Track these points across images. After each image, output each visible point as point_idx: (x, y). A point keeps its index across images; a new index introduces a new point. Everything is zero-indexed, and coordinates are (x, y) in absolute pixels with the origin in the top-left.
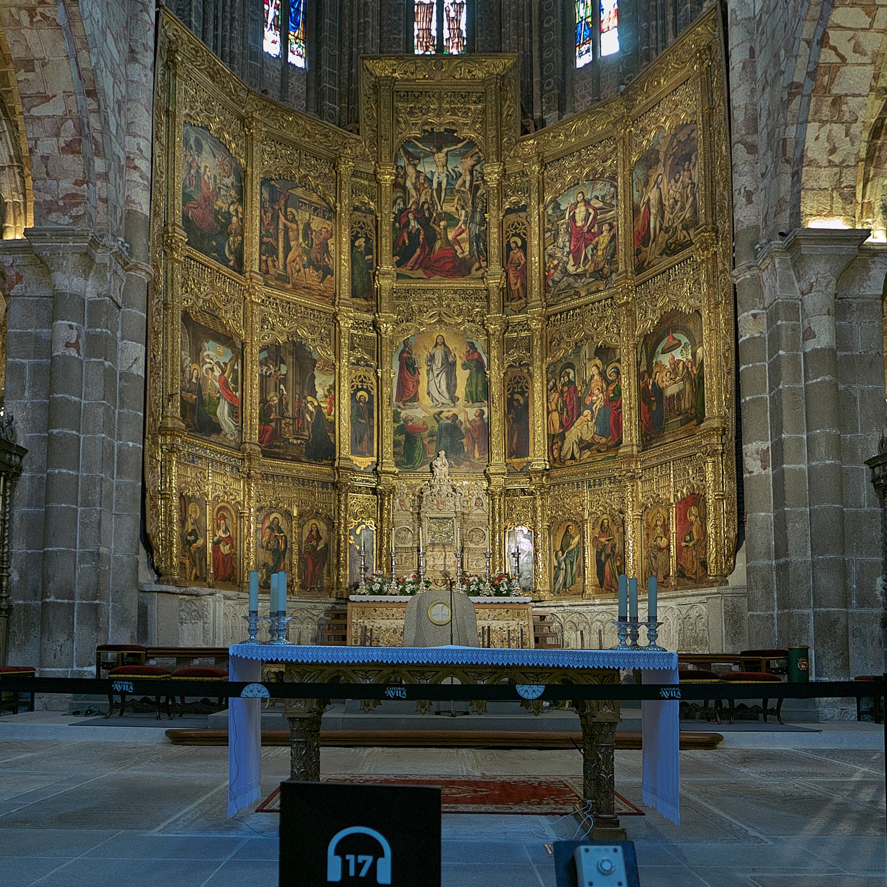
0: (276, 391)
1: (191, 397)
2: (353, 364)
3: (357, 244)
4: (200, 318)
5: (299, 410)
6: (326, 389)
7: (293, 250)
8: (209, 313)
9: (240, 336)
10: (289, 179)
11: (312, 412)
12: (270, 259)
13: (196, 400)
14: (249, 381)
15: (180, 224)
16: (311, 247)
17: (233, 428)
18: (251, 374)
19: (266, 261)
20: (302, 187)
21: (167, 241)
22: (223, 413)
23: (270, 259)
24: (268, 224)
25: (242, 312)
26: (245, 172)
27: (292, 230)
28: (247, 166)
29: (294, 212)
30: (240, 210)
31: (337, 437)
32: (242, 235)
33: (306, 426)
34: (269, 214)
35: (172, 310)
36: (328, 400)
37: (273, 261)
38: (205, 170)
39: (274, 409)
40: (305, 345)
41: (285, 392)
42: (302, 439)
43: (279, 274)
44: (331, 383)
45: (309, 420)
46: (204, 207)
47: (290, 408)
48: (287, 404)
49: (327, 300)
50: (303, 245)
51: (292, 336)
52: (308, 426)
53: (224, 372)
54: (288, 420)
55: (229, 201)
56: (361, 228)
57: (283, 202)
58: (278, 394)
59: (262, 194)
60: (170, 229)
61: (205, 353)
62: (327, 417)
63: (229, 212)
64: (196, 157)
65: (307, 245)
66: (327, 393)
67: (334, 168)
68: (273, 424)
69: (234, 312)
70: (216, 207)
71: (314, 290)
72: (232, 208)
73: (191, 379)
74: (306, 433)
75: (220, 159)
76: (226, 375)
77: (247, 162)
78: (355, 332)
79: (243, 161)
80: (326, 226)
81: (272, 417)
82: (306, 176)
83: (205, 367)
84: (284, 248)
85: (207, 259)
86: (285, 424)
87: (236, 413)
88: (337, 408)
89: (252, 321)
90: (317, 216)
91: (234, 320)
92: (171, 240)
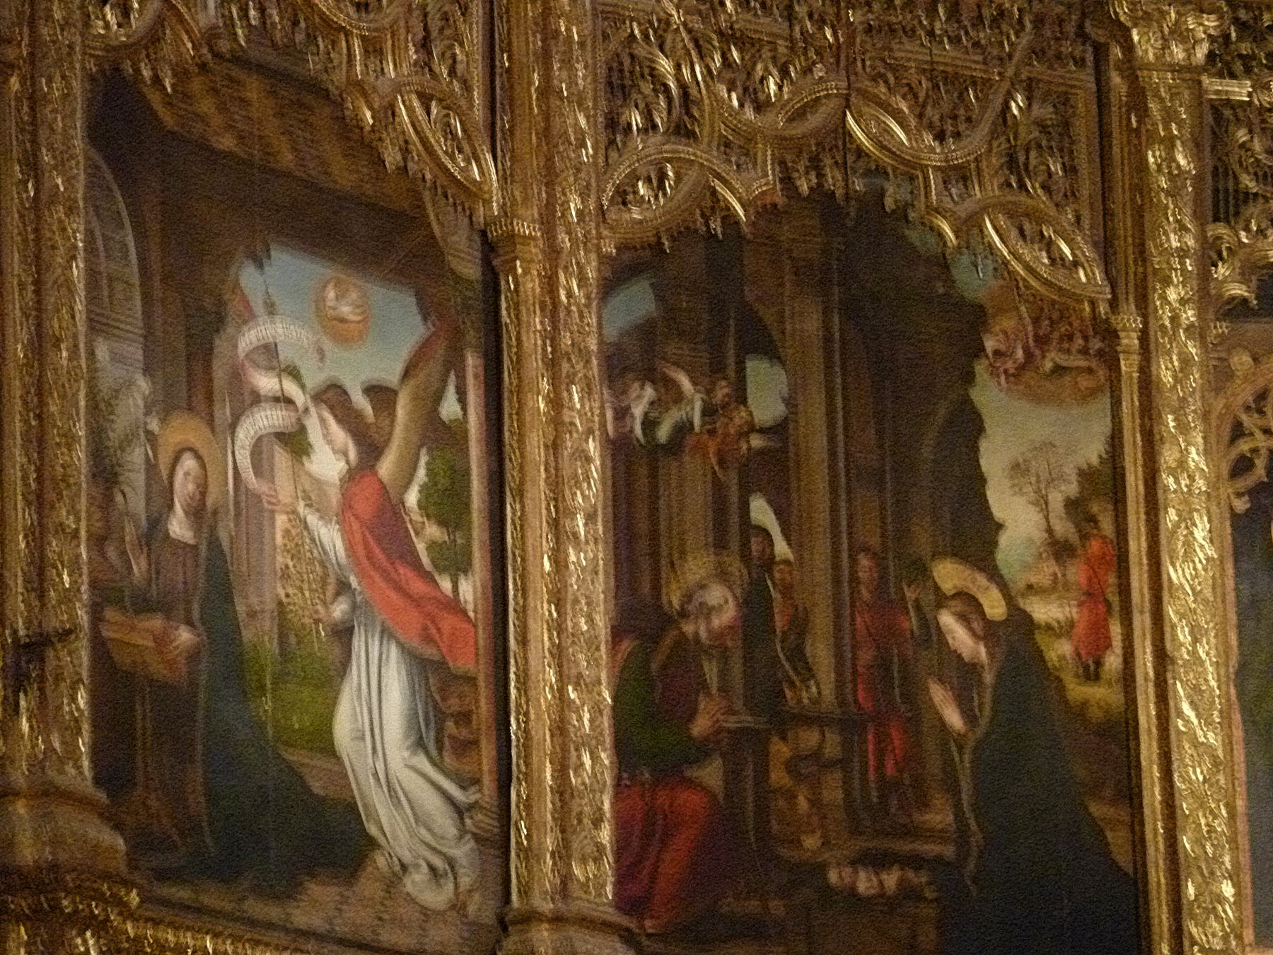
0: (720, 544)
1: (162, 641)
2: (1236, 310)
4: (206, 106)
5: (883, 665)
6: (1056, 499)
8: (261, 69)
9: (469, 193)
11: (970, 670)
13: (193, 656)
14: (538, 489)
17: (445, 822)
18: (555, 447)
22: (375, 729)
25: (474, 35)
31: (1155, 827)
33: (934, 765)
35: (30, 80)
36: (1076, 572)
39: (711, 670)
40: (902, 214)
41: (781, 548)
42: (916, 862)
44: (1093, 452)
45: (954, 718)
47: (820, 652)
48: (800, 624)
51: (815, 165)
52: (948, 762)
53: (370, 447)
54: (810, 738)
58: (735, 566)
61: (249, 338)
62: (1077, 691)
66: (1063, 528)
68: (711, 774)
69: (425, 45)
73: (156, 523)
74: (939, 816)
76: (387, 467)
78: (1240, 90)
81: (701, 726)
83: (246, 434)
86: (792, 766)
87: (464, 718)
88: (1142, 621)
89: (547, 91)
91: (425, 100)
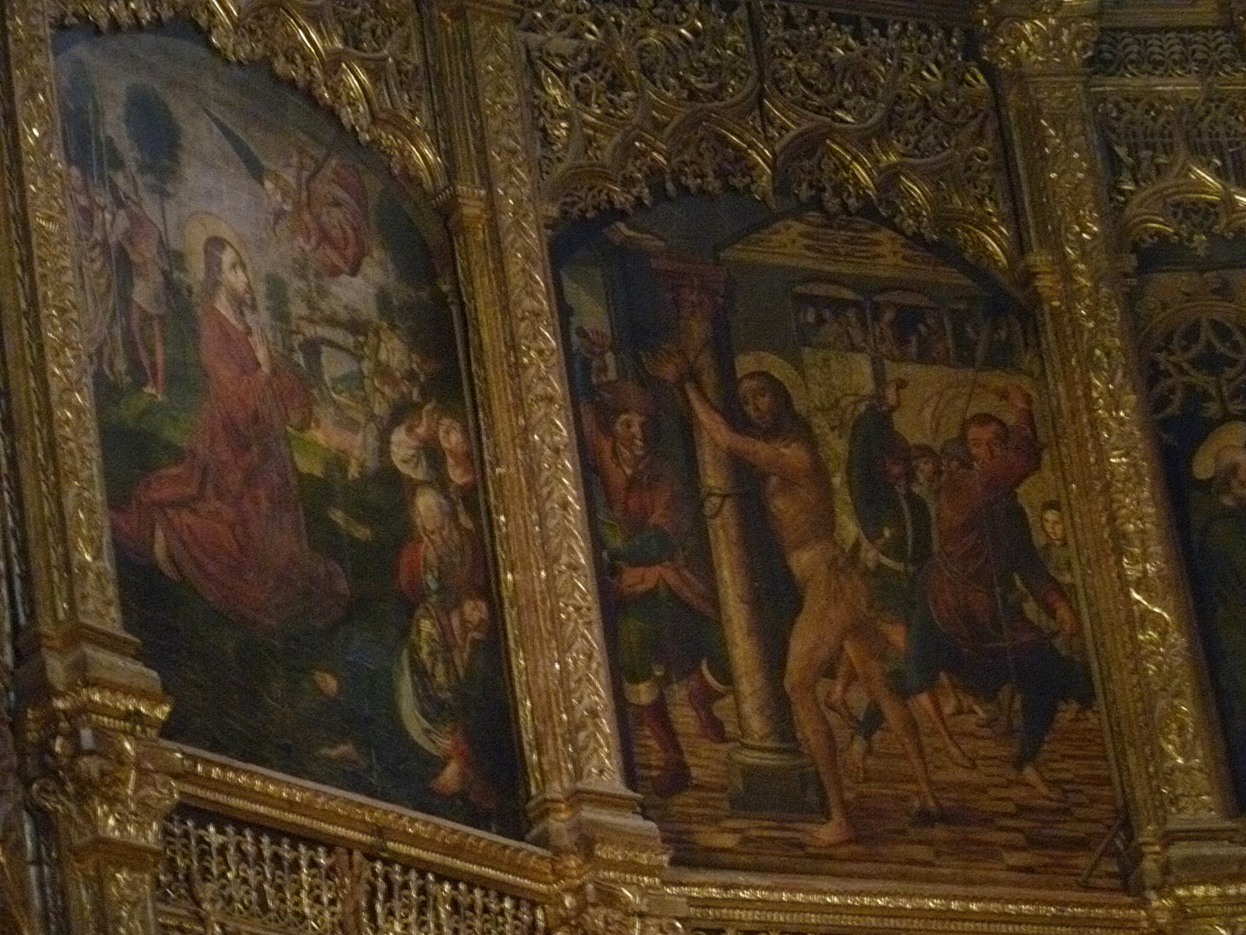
3: (1203, 467)
7: (814, 602)
10: (713, 184)
12: (679, 693)
15: (112, 621)
16: (922, 554)
19: (659, 710)
20: (798, 211)
21: (44, 747)
23: (679, 693)
24: (632, 483)
26: (447, 211)
27: (788, 484)
28: (451, 173)
29: (778, 368)
30: (452, 439)
32: (489, 591)
34: (632, 423)
37: (704, 700)
38: (213, 266)
43: (749, 772)
46: (235, 479)
49: (1083, 861)
50: (870, 555)
55: (380, 408)
56: (1211, 362)
57: (697, 329)
59: (564, 312)
60: (57, 669)
63: (389, 478)
64: (151, 208)
65: (895, 549)
67: (971, 51)
70: (309, 465)
71: (987, 820)
72: (402, 445)
75: (289, 176)
77: (449, 155)
79: (424, 155)
80: (988, 404)
82: (810, 145)
84: (757, 601)
85: (298, 789)
90: (924, 357)
92: (73, 736)
